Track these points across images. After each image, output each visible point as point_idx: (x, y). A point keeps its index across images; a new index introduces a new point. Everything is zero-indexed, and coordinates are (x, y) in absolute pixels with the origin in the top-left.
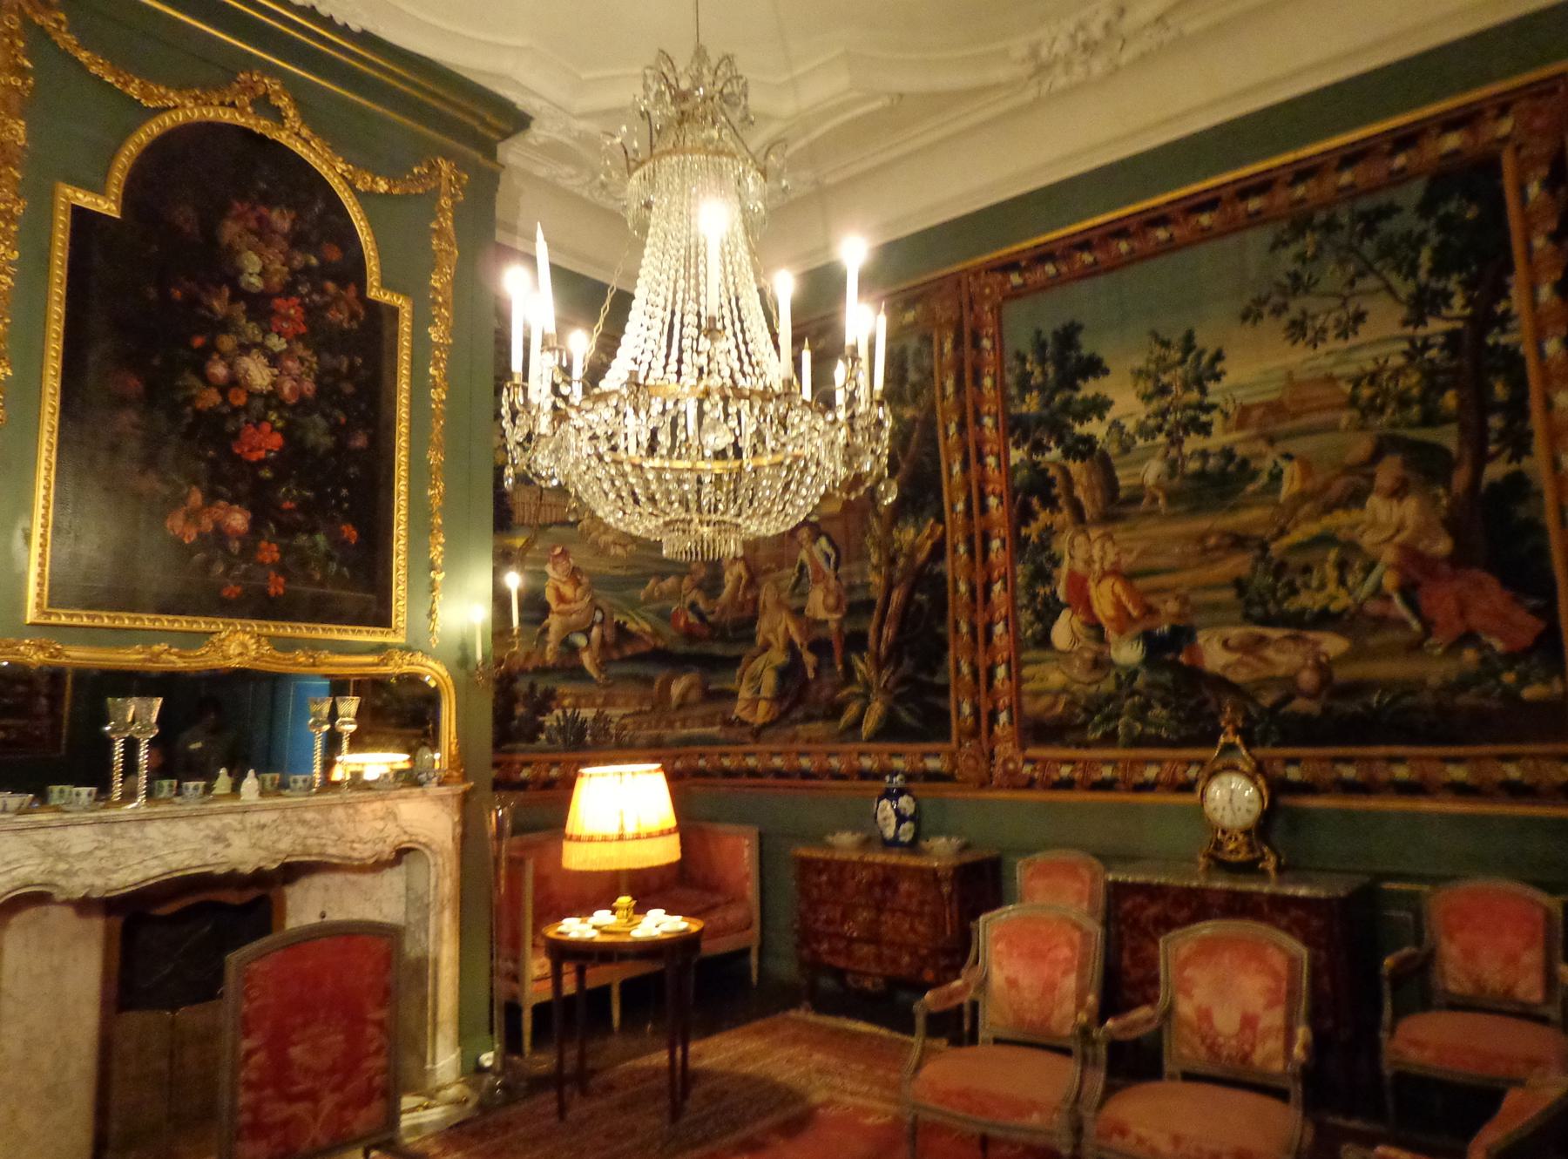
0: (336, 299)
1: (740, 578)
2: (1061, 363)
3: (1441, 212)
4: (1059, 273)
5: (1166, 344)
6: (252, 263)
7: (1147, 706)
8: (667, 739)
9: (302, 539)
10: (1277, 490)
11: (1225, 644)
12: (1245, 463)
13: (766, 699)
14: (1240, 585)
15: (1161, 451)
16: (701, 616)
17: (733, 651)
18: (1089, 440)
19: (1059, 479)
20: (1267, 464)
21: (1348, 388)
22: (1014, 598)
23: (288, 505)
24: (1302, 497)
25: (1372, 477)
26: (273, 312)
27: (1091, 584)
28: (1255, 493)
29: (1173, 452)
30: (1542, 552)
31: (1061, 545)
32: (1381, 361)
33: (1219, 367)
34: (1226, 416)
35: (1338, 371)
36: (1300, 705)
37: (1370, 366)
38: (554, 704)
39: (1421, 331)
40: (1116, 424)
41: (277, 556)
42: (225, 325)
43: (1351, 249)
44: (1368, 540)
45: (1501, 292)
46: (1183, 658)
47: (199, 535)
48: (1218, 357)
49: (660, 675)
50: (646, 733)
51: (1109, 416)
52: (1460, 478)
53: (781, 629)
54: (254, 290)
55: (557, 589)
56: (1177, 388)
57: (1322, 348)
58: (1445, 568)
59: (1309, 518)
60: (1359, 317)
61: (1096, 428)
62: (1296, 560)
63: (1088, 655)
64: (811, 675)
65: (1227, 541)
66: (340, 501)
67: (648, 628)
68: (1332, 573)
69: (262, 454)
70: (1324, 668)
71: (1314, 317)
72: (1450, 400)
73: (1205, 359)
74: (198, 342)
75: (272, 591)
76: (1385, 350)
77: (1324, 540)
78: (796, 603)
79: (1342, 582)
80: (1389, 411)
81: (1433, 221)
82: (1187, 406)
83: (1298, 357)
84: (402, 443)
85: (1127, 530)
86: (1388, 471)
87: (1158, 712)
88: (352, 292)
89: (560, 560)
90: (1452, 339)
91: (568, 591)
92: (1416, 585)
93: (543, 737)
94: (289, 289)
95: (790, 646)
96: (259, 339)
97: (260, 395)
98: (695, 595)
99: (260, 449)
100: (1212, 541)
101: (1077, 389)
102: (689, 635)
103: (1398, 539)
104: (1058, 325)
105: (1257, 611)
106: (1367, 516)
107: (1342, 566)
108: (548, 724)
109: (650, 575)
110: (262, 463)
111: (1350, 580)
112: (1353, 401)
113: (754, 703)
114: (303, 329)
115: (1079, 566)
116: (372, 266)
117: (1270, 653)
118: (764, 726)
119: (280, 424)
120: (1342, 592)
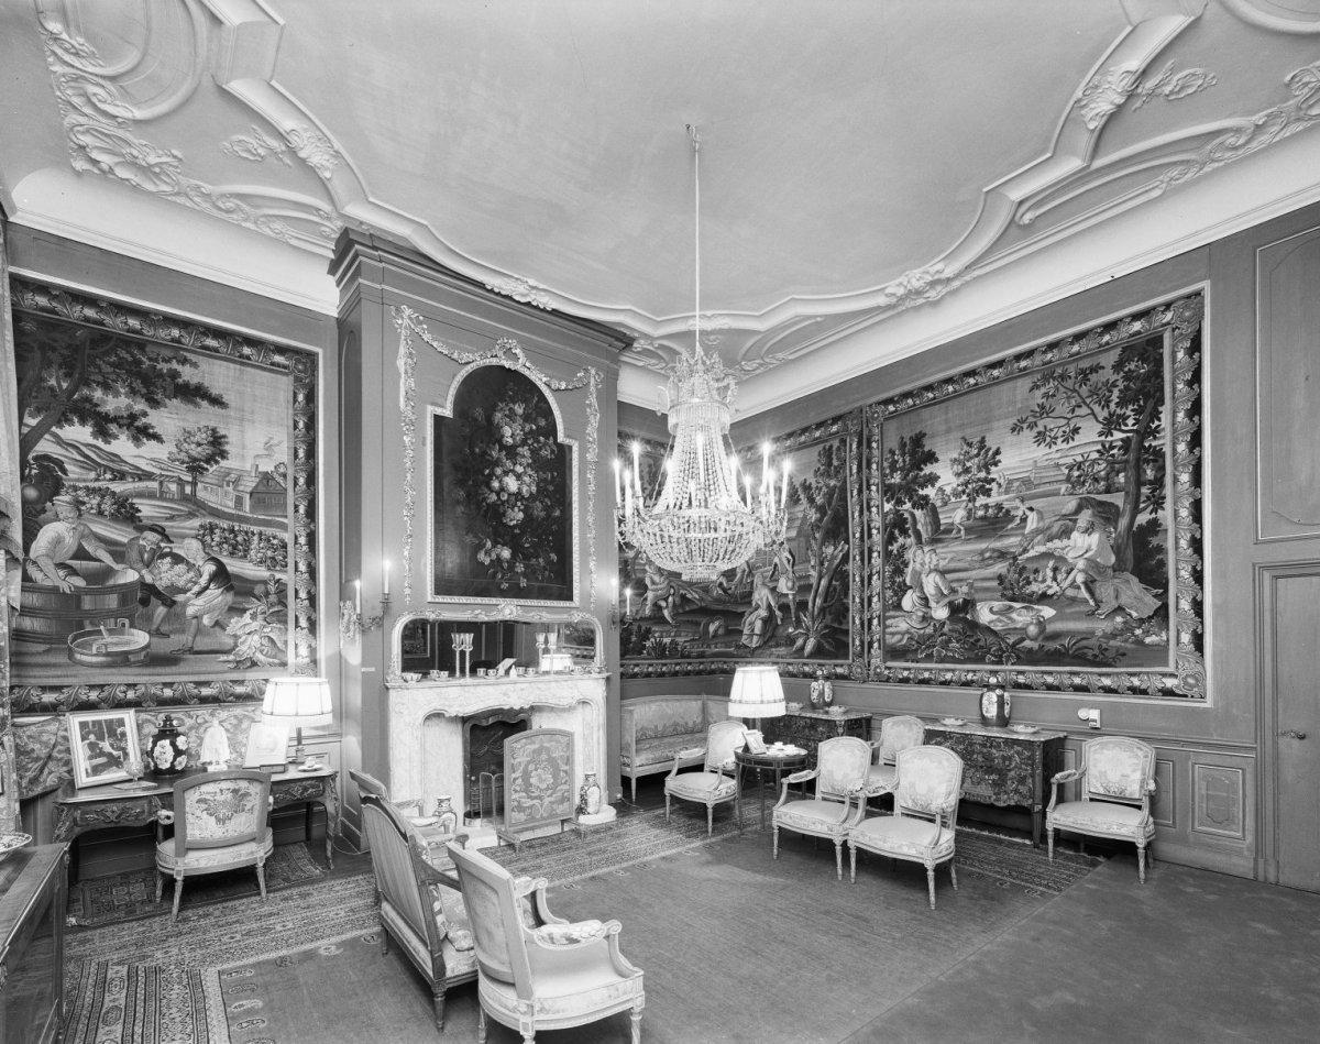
2: (913, 454)
3: (1126, 369)
4: (915, 405)
5: (970, 445)
7: (949, 641)
10: (1025, 527)
11: (991, 610)
12: (1008, 511)
14: (1001, 578)
15: (964, 504)
18: (926, 498)
19: (910, 519)
20: (1020, 513)
21: (1067, 471)
22: (883, 583)
24: (1037, 532)
25: (1075, 521)
27: (923, 576)
28: (1012, 528)
29: (970, 505)
30: (1162, 564)
31: (909, 555)
32: (1086, 455)
33: (998, 458)
34: (1000, 486)
35: (1062, 461)
36: (1027, 643)
37: (1079, 459)
39: (1110, 438)
40: (940, 489)
43: (1074, 391)
44: (1070, 556)
45: (1156, 415)
46: (968, 617)
48: (998, 452)
51: (937, 485)
52: (1123, 522)
56: (974, 470)
57: (1054, 448)
58: (1110, 571)
59: (1038, 544)
60: (1076, 430)
61: (930, 491)
62: (1030, 566)
63: (920, 614)
65: (996, 554)
68: (1050, 574)
70: (1041, 624)
71: (1051, 430)
72: (1121, 478)
73: (990, 453)
76: (1088, 449)
77: (1047, 555)
79: (1055, 579)
80: (1087, 485)
81: (1122, 374)
82: (979, 480)
83: (1040, 452)
85: (943, 547)
86: (1085, 517)
87: (954, 644)
90: (1126, 441)
92: (1093, 581)
100: (987, 555)
101: (921, 470)
103: (1086, 556)
104: (913, 434)
105: (1009, 593)
106: (1071, 542)
107: (1055, 570)
111: (1059, 578)
112: (1068, 479)
115: (918, 567)
117: (1014, 615)
120: (1054, 584)
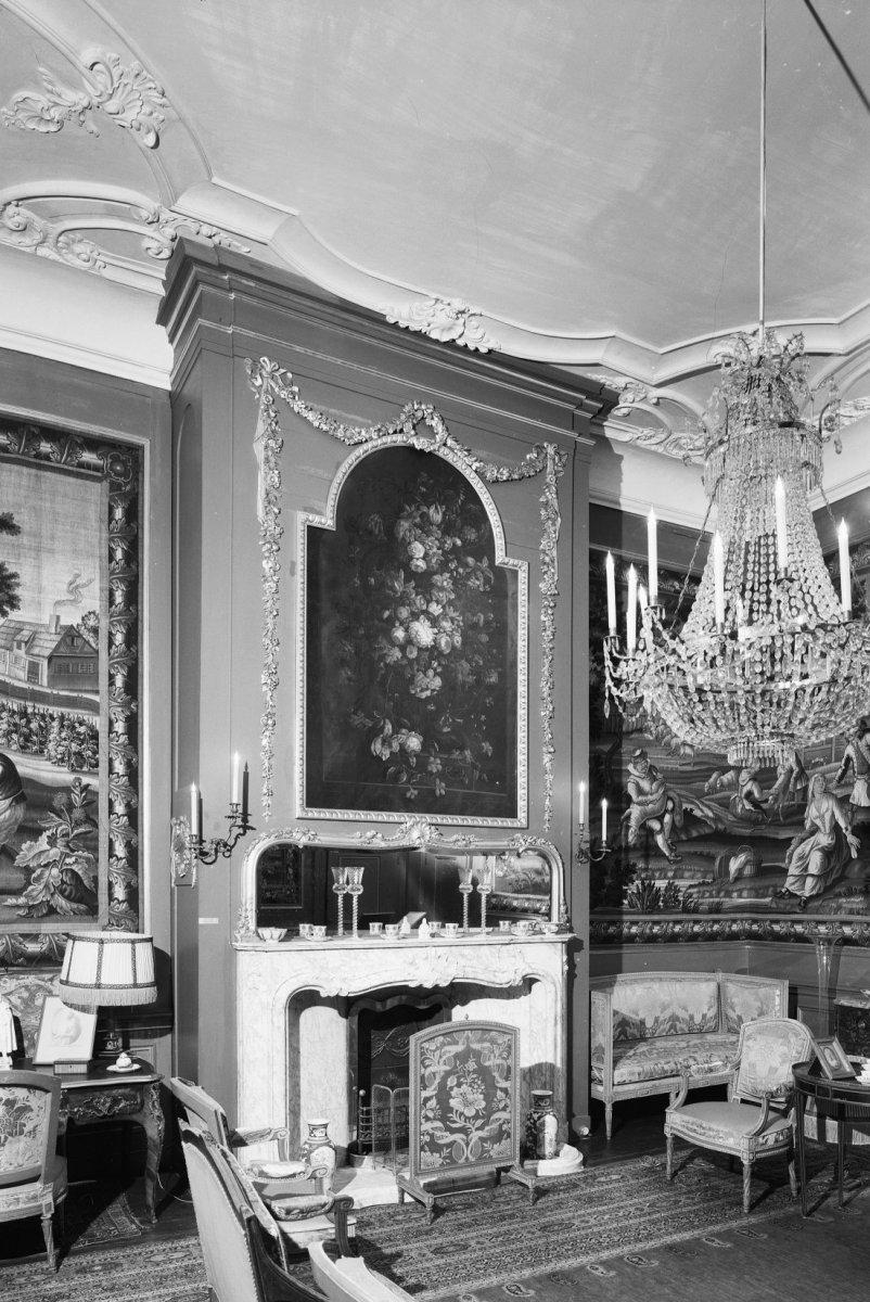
0: (475, 570)
1: (791, 771)
6: (418, 550)
8: (726, 906)
9: (456, 754)
13: (812, 875)
16: (756, 804)
17: (783, 835)
23: (446, 730)
26: (433, 585)
38: (635, 876)
41: (440, 767)
42: (403, 600)
47: (391, 753)
49: (720, 853)
50: (707, 901)
53: (827, 817)
54: (420, 570)
55: (637, 785)
64: (854, 855)
66: (480, 726)
67: (711, 814)
69: (428, 693)
74: (386, 614)
75: (438, 792)
78: (840, 793)
84: (522, 678)
88: (485, 563)
89: (639, 760)
91: (645, 785)
93: (626, 902)
94: (443, 567)
95: (836, 828)
96: (424, 607)
97: (427, 649)
98: (750, 786)
99: (427, 689)
102: (745, 819)
108: (630, 892)
109: (713, 770)
113: (802, 878)
114: (453, 596)
116: (499, 542)
118: (811, 898)
119: (439, 670)
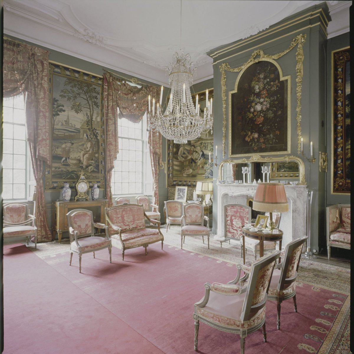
9: (268, 136)
66: (275, 126)
69: (260, 122)
75: (263, 147)
110: (260, 124)
119: (263, 116)
